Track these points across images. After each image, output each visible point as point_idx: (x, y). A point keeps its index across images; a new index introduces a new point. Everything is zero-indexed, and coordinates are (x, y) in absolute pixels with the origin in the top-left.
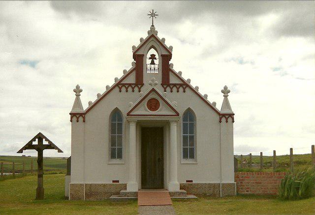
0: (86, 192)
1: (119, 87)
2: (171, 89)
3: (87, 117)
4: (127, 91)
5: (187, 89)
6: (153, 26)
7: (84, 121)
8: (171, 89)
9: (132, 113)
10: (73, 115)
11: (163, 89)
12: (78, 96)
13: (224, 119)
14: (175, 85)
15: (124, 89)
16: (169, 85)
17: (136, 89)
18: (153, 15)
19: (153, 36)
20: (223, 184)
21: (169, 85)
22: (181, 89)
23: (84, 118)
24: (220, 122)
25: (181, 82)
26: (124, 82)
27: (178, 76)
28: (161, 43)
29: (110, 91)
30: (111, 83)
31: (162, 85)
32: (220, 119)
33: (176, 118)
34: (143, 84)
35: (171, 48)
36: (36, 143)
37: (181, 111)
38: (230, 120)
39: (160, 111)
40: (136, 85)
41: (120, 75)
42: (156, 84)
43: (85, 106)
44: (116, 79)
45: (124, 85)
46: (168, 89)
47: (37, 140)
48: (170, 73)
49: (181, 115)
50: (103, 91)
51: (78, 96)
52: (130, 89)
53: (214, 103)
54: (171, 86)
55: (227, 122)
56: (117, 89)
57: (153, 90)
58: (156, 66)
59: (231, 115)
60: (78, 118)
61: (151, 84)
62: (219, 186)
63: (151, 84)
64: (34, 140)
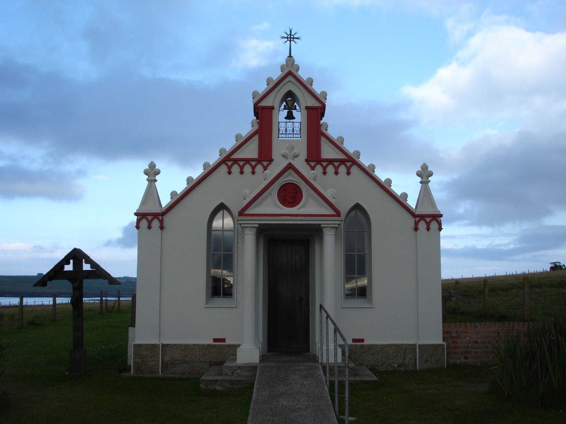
0: (162, 359)
1: (227, 165)
2: (325, 168)
3: (167, 219)
4: (242, 172)
5: (354, 169)
6: (290, 56)
7: (162, 228)
8: (325, 168)
9: (248, 212)
10: (141, 216)
11: (308, 167)
12: (152, 181)
13: (422, 225)
14: (331, 161)
15: (236, 169)
16: (319, 161)
17: (259, 168)
18: (291, 38)
19: (290, 73)
20: (421, 346)
21: (319, 161)
22: (342, 169)
23: (161, 222)
24: (416, 229)
25: (343, 157)
26: (235, 156)
27: (337, 145)
28: (306, 87)
29: (209, 173)
30: (214, 158)
31: (308, 161)
32: (416, 224)
33: (336, 222)
34: (271, 160)
35: (324, 94)
36: (69, 268)
37: (344, 209)
38: (434, 225)
39: (303, 206)
40: (259, 161)
41: (229, 145)
42: (296, 156)
43: (165, 200)
44: (222, 151)
45: (236, 161)
46: (319, 169)
47: (71, 261)
48: (323, 139)
49: (343, 214)
50: (197, 173)
51: (152, 181)
52: (248, 169)
53: (405, 195)
54: (325, 164)
55: (428, 229)
56: (224, 168)
57: (290, 166)
58: (297, 125)
59: (436, 218)
60: (150, 223)
61: (284, 156)
62: (414, 350)
63: (284, 156)
64: (66, 261)
